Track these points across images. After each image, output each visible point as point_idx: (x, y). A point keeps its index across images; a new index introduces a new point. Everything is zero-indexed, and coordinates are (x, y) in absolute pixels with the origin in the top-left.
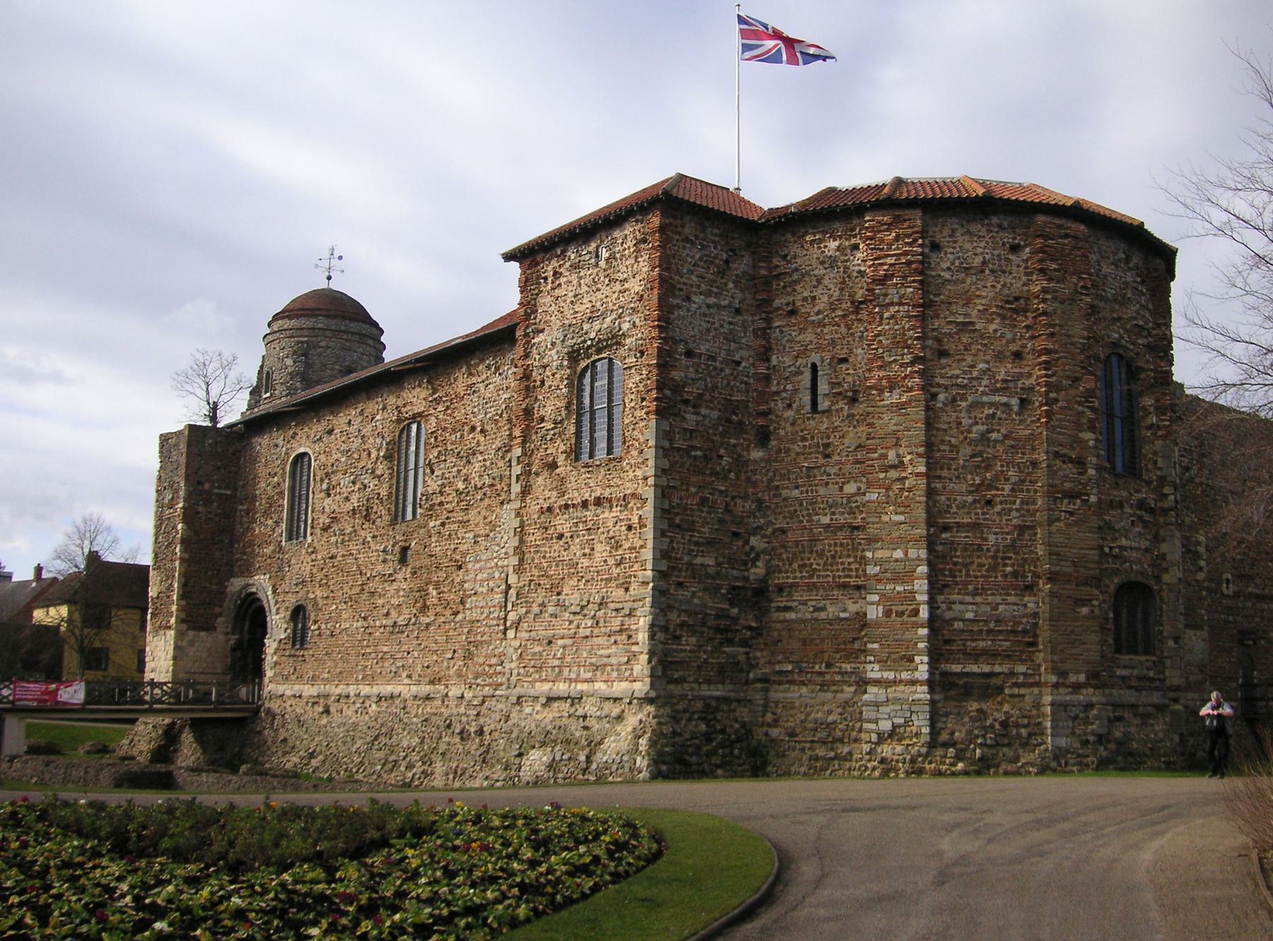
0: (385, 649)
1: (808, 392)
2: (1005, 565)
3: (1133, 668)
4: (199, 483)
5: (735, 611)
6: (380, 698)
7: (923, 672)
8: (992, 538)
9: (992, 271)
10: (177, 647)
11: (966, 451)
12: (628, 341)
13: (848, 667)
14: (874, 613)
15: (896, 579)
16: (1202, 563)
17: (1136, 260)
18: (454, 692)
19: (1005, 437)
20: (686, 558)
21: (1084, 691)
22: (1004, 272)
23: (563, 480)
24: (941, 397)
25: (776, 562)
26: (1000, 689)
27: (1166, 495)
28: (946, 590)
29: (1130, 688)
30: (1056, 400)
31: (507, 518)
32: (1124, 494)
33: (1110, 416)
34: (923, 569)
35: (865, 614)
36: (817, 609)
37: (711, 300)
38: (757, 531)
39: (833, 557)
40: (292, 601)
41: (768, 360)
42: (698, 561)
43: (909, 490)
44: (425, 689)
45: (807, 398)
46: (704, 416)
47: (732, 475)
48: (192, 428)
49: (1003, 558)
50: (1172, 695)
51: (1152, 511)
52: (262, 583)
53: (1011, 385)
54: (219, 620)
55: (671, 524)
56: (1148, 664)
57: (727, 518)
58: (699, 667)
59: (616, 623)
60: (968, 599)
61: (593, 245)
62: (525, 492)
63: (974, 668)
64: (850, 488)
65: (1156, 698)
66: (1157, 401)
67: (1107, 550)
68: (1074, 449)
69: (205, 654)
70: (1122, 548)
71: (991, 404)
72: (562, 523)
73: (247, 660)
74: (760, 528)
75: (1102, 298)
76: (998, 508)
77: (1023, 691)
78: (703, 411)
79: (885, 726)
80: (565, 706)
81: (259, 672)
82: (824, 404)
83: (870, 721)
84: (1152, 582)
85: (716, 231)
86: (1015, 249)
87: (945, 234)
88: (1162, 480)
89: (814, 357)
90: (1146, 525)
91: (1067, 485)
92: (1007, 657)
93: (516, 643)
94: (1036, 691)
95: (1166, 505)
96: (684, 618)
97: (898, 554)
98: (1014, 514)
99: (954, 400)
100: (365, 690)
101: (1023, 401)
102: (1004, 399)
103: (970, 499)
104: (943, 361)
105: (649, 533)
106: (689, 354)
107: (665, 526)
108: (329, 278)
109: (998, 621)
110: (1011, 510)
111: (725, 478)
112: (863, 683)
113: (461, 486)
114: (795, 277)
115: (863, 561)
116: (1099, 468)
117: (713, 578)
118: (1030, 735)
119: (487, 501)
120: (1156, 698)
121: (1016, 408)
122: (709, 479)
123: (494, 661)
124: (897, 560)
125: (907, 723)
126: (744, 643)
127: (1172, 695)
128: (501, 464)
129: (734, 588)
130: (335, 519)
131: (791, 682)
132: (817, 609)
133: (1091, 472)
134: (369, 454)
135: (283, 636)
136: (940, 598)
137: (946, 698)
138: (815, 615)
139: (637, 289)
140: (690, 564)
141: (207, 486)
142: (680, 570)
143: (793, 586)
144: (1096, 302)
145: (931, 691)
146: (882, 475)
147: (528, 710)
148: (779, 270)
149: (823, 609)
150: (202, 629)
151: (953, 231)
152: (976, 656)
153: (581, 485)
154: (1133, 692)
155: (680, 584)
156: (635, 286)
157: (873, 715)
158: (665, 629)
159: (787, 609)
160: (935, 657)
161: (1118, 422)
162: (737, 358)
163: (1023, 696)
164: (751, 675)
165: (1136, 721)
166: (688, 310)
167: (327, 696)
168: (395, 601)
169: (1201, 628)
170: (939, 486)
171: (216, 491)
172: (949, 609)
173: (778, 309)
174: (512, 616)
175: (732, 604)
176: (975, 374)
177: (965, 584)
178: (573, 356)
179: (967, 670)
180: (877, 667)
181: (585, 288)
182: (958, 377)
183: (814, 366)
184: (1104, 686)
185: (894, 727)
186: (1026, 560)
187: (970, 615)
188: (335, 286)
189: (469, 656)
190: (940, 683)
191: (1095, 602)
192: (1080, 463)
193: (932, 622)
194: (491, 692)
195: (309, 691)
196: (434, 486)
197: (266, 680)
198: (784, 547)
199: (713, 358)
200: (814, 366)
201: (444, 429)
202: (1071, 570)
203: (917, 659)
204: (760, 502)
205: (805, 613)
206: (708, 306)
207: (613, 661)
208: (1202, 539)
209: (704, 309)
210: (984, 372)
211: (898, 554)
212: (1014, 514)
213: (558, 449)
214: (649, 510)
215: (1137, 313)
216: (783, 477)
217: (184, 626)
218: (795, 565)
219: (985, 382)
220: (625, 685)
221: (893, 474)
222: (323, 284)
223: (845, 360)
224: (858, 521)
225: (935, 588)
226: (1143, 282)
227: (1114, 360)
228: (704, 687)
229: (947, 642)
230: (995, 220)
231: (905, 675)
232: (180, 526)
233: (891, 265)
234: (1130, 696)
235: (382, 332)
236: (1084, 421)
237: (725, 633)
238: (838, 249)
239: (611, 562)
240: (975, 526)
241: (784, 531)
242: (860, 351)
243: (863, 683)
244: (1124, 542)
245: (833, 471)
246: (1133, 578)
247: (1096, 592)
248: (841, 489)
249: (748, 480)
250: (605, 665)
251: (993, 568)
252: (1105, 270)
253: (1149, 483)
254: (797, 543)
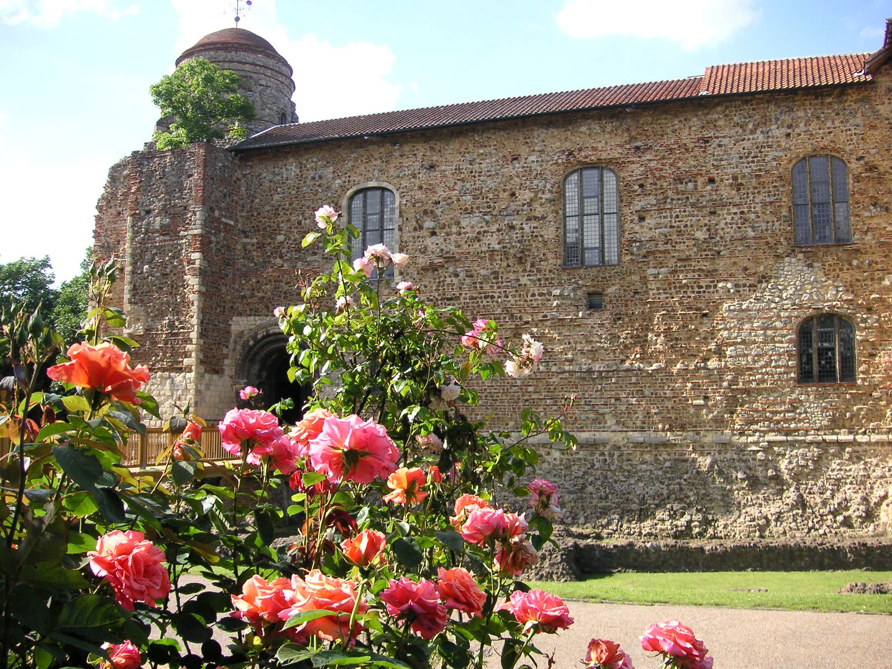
54: (226, 362)
69: (217, 400)
108: (237, 19)
141: (217, 213)
171: (223, 220)
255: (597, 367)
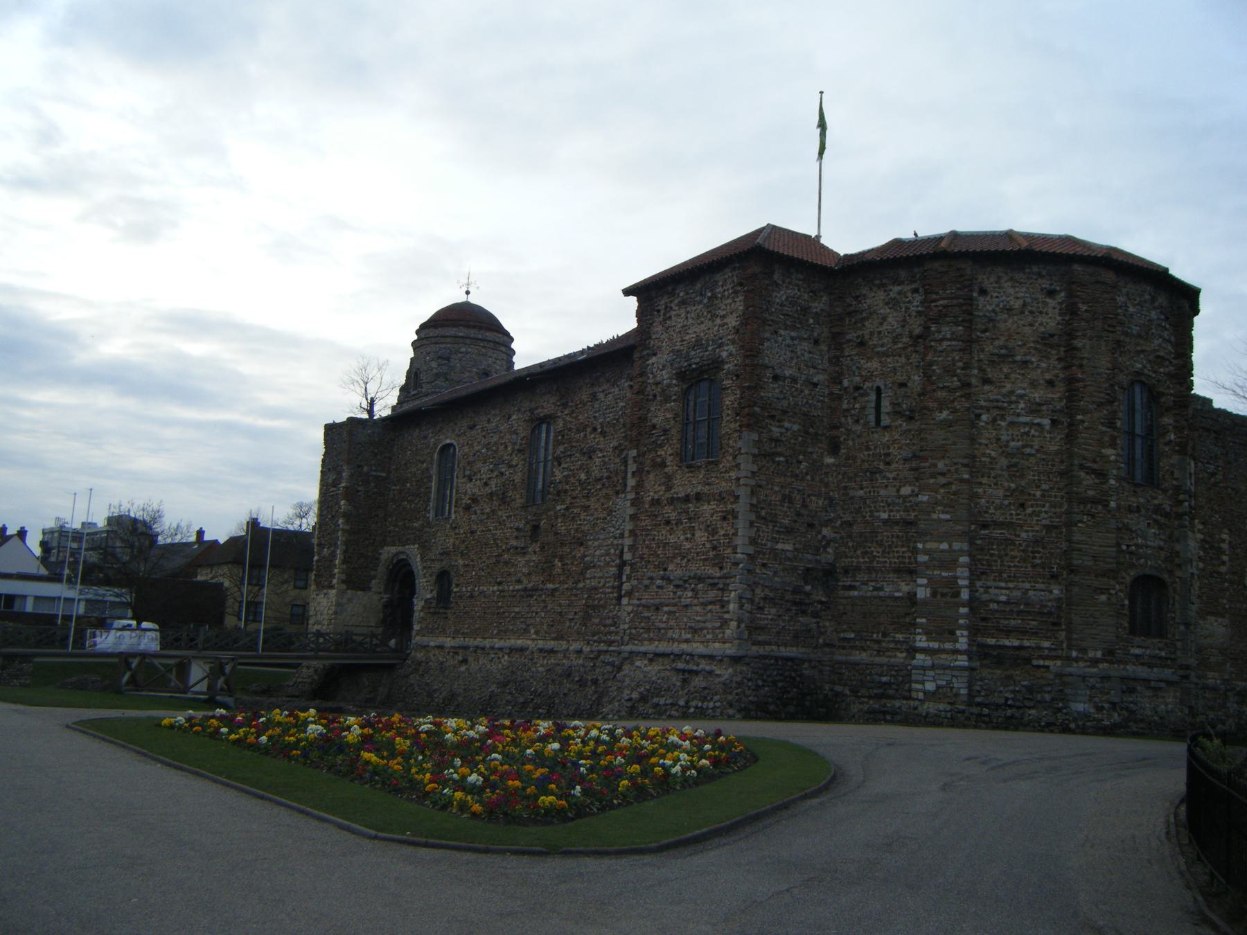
0: (517, 609)
1: (873, 411)
2: (1034, 558)
3: (1146, 648)
4: (359, 466)
5: (808, 588)
6: (512, 650)
7: (963, 643)
8: (1024, 535)
9: (1031, 312)
10: (338, 604)
11: (1004, 462)
12: (726, 367)
13: (900, 637)
14: (922, 593)
15: (943, 566)
16: (1225, 558)
17: (1162, 300)
18: (575, 646)
19: (1038, 451)
20: (769, 544)
21: (1101, 666)
22: (1041, 313)
23: (669, 478)
24: (984, 417)
25: (843, 549)
26: (1028, 661)
27: (1181, 502)
28: (984, 577)
29: (1143, 664)
30: (1083, 421)
31: (624, 506)
32: (1142, 500)
33: (1131, 434)
34: (964, 559)
35: (915, 594)
36: (876, 589)
37: (793, 334)
38: (828, 523)
39: (890, 546)
40: (437, 566)
41: (841, 383)
42: (780, 546)
43: (954, 494)
44: (551, 644)
45: (872, 418)
46: (787, 429)
47: (809, 477)
48: (351, 420)
49: (1033, 552)
50: (1181, 672)
51: (1167, 515)
52: (413, 552)
53: (1044, 408)
55: (759, 517)
56: (1160, 645)
57: (805, 512)
58: (778, 633)
59: (712, 594)
60: (1003, 584)
61: (699, 286)
62: (639, 486)
63: (1007, 643)
64: (906, 490)
65: (1168, 673)
66: (1176, 421)
67: (1124, 547)
68: (1095, 461)
70: (1137, 545)
71: (1026, 424)
72: (670, 513)
73: (398, 614)
74: (830, 520)
75: (1126, 334)
76: (1029, 511)
77: (1047, 663)
78: (786, 425)
79: (930, 686)
80: (666, 661)
81: (410, 628)
82: (886, 421)
83: (917, 682)
84: (1165, 576)
85: (800, 276)
86: (1051, 293)
87: (992, 280)
88: (1178, 489)
89: (879, 382)
90: (1160, 526)
91: (1091, 493)
92: (1034, 634)
93: (629, 609)
94: (1059, 663)
95: (1180, 510)
96: (767, 592)
97: (944, 546)
98: (1043, 515)
99: (994, 420)
100: (498, 643)
101: (1053, 422)
102: (1037, 421)
103: (1006, 502)
104: (987, 388)
105: (741, 524)
106: (776, 378)
107: (753, 517)
108: (468, 293)
109: (1026, 604)
110: (1040, 512)
111: (802, 480)
112: (913, 651)
113: (583, 476)
114: (864, 315)
115: (915, 551)
116: (1118, 479)
117: (790, 559)
118: (1053, 699)
119: (604, 491)
120: (1168, 673)
121: (1048, 427)
122: (789, 480)
123: (609, 622)
124: (942, 551)
125: (949, 682)
126: (815, 615)
127: (1181, 672)
128: (618, 460)
129: (808, 570)
130: (475, 500)
131: (854, 648)
132: (876, 589)
133: (1112, 482)
134: (506, 447)
135: (429, 596)
136: (979, 584)
137: (982, 666)
138: (875, 593)
139: (734, 324)
140: (773, 550)
141: (365, 469)
142: (764, 554)
143: (857, 569)
144: (1122, 338)
145: (970, 659)
146: (932, 481)
147: (638, 663)
148: (852, 309)
149: (881, 589)
150: (363, 590)
151: (999, 278)
152: (1008, 632)
153: (685, 484)
154: (1146, 669)
155: (764, 565)
156: (732, 321)
157: (920, 678)
158: (752, 601)
159: (852, 588)
160: (974, 631)
161: (1138, 441)
162: (815, 380)
163: (1048, 667)
164: (821, 641)
165: (1149, 693)
166: (776, 342)
167: (466, 648)
168: (525, 570)
169: (1222, 616)
170: (980, 490)
172: (986, 592)
173: (849, 341)
174: (626, 587)
175: (806, 583)
176: (1014, 398)
177: (1001, 573)
178: (681, 375)
179: (1001, 643)
180: (924, 638)
181: (690, 321)
182: (997, 401)
183: (878, 390)
184: (1119, 662)
185: (938, 687)
186: (1052, 554)
187: (1003, 598)
188: (474, 299)
189: (586, 618)
190: (980, 653)
191: (1112, 592)
192: (1102, 475)
193: (972, 603)
194: (605, 648)
195: (449, 642)
196: (559, 475)
197: (414, 633)
198: (850, 536)
199: (794, 380)
200: (878, 390)
201: (570, 429)
202: (1090, 563)
203: (958, 633)
204: (831, 500)
205: (867, 590)
206: (792, 338)
207: (708, 625)
208: (1224, 536)
209: (788, 341)
210: (1022, 396)
211: (944, 546)
212: (1043, 515)
213: (666, 452)
214: (742, 507)
215: (1160, 345)
216: (850, 479)
217: (344, 586)
218: (859, 552)
219: (1022, 405)
220: (717, 645)
221: (942, 480)
222: (461, 298)
223: (903, 385)
224: (912, 515)
225: (975, 575)
226: (1167, 318)
227: (1137, 389)
228: (782, 649)
229: (984, 619)
230: (1035, 269)
231: (948, 646)
232: (342, 502)
233: (944, 307)
234: (1142, 672)
235: (512, 340)
236: (1106, 439)
237: (801, 606)
238: (900, 293)
239: (708, 545)
240: (1009, 525)
241: (850, 524)
242: (916, 378)
243: (913, 651)
244: (1140, 541)
245: (890, 476)
246: (1148, 572)
247: (1112, 582)
248: (898, 491)
249: (821, 481)
250: (702, 629)
251: (1024, 560)
252: (1131, 309)
253: (1165, 491)
254: (861, 534)
255: (530, 586)
